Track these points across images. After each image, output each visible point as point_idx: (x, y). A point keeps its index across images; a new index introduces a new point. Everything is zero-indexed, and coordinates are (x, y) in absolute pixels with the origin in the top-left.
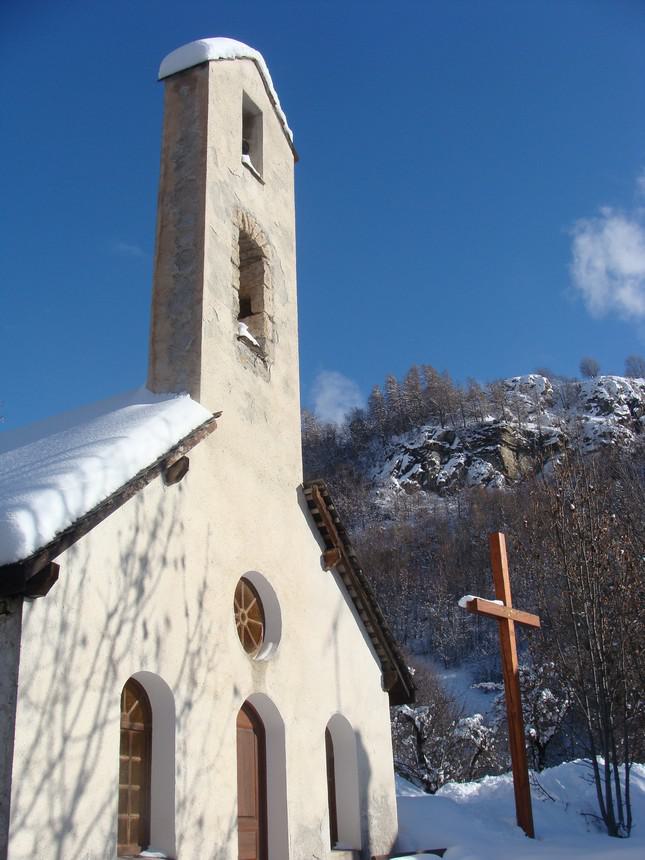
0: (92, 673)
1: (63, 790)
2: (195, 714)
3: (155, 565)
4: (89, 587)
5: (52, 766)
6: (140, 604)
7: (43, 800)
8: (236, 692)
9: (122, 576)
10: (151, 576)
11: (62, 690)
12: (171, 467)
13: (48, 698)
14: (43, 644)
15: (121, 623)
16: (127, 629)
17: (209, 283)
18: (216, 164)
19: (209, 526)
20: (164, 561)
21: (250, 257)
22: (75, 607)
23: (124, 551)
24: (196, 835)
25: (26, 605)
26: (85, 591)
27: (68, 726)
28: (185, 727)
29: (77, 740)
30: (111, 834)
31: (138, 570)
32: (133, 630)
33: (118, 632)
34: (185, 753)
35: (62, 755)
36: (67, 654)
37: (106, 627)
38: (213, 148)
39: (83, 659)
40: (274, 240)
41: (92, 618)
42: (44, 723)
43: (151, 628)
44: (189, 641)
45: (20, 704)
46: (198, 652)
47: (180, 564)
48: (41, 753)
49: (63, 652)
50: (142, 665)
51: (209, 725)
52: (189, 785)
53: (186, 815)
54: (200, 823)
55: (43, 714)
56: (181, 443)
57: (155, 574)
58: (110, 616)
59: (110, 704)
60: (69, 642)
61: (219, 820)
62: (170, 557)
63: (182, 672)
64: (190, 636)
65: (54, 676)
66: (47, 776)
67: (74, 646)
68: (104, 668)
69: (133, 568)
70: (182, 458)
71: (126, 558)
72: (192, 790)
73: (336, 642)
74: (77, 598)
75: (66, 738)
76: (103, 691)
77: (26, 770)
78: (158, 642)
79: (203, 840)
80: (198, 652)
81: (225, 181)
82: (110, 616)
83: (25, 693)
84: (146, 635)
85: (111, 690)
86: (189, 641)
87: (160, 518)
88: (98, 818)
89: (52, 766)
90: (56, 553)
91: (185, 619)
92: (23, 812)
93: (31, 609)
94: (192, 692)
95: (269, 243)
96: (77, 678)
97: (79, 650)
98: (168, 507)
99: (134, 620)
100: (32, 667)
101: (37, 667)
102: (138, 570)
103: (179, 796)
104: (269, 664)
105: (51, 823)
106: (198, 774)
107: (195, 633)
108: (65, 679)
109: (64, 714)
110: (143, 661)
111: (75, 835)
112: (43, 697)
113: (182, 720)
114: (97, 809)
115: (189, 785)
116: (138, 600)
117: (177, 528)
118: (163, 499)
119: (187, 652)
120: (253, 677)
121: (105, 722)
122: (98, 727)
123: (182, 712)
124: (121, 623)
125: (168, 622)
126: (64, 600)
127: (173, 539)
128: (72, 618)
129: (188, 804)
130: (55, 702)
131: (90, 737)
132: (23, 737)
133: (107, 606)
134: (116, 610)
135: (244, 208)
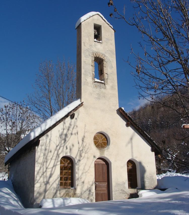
0: (53, 157)
1: (46, 177)
2: (81, 162)
3: (69, 135)
4: (51, 142)
5: (44, 173)
6: (65, 143)
7: (42, 179)
8: (94, 157)
9: (60, 139)
10: (68, 138)
11: (46, 160)
12: (71, 115)
13: (42, 162)
14: (41, 153)
15: (60, 147)
16: (61, 148)
17: (84, 74)
18: (85, 46)
19: (85, 125)
20: (72, 134)
21: (99, 62)
22: (48, 146)
23: (60, 134)
24: (82, 185)
25: (36, 147)
26: (51, 143)
27: (47, 166)
28: (78, 164)
29: (49, 168)
30: (58, 184)
31: (64, 138)
32: (63, 148)
33: (59, 149)
34: (78, 170)
35: (46, 171)
36: (47, 154)
37: (56, 148)
38: (84, 43)
39: (50, 155)
40: (107, 55)
41: (53, 147)
42: (42, 166)
43: (68, 147)
44: (79, 148)
45: (36, 163)
46: (82, 150)
47: (76, 134)
48: (41, 170)
49: (46, 154)
50: (66, 154)
51: (86, 164)
52: (80, 176)
53: (79, 181)
54: (83, 182)
55: (41, 164)
56: (73, 110)
57: (69, 137)
58: (57, 146)
59: (57, 162)
60: (47, 152)
61: (89, 182)
62: (73, 133)
63: (77, 154)
64: (80, 147)
65: (44, 158)
66: (43, 174)
67: (48, 153)
68: (56, 156)
69: (63, 136)
70: (73, 114)
71: (61, 135)
72: (81, 176)
73: (132, 143)
74: (49, 144)
75: (47, 168)
76: (55, 160)
77: (38, 173)
78: (70, 149)
79: (84, 186)
80: (82, 150)
81: (88, 49)
82: (57, 146)
83: (37, 161)
84: (67, 148)
85: (58, 159)
86: (79, 148)
87: (70, 126)
88: (55, 181)
89: (44, 173)
90: (40, 138)
91: (78, 144)
92: (37, 180)
93: (38, 148)
94: (80, 158)
95: (105, 56)
96: (49, 158)
97: (49, 153)
98: (73, 123)
99: (64, 146)
100: (38, 157)
101: (39, 157)
102: (64, 138)
103: (77, 177)
104: (106, 150)
105: (44, 182)
106: (83, 173)
107: (81, 146)
108: (46, 158)
109: (46, 164)
110: (66, 153)
111: (49, 184)
112: (41, 161)
113: (78, 163)
114: (55, 180)
115: (80, 176)
116: (64, 142)
117: (75, 127)
118: (71, 122)
119: (79, 150)
120: (100, 153)
121: (56, 165)
122: (55, 166)
123: (78, 162)
124: (60, 147)
125: (73, 145)
126: (45, 145)
127: (74, 129)
128: (48, 148)
129: (79, 179)
130: (44, 162)
131: (52, 168)
132: (37, 168)
133: (56, 145)
134: (59, 145)
135: (96, 52)
